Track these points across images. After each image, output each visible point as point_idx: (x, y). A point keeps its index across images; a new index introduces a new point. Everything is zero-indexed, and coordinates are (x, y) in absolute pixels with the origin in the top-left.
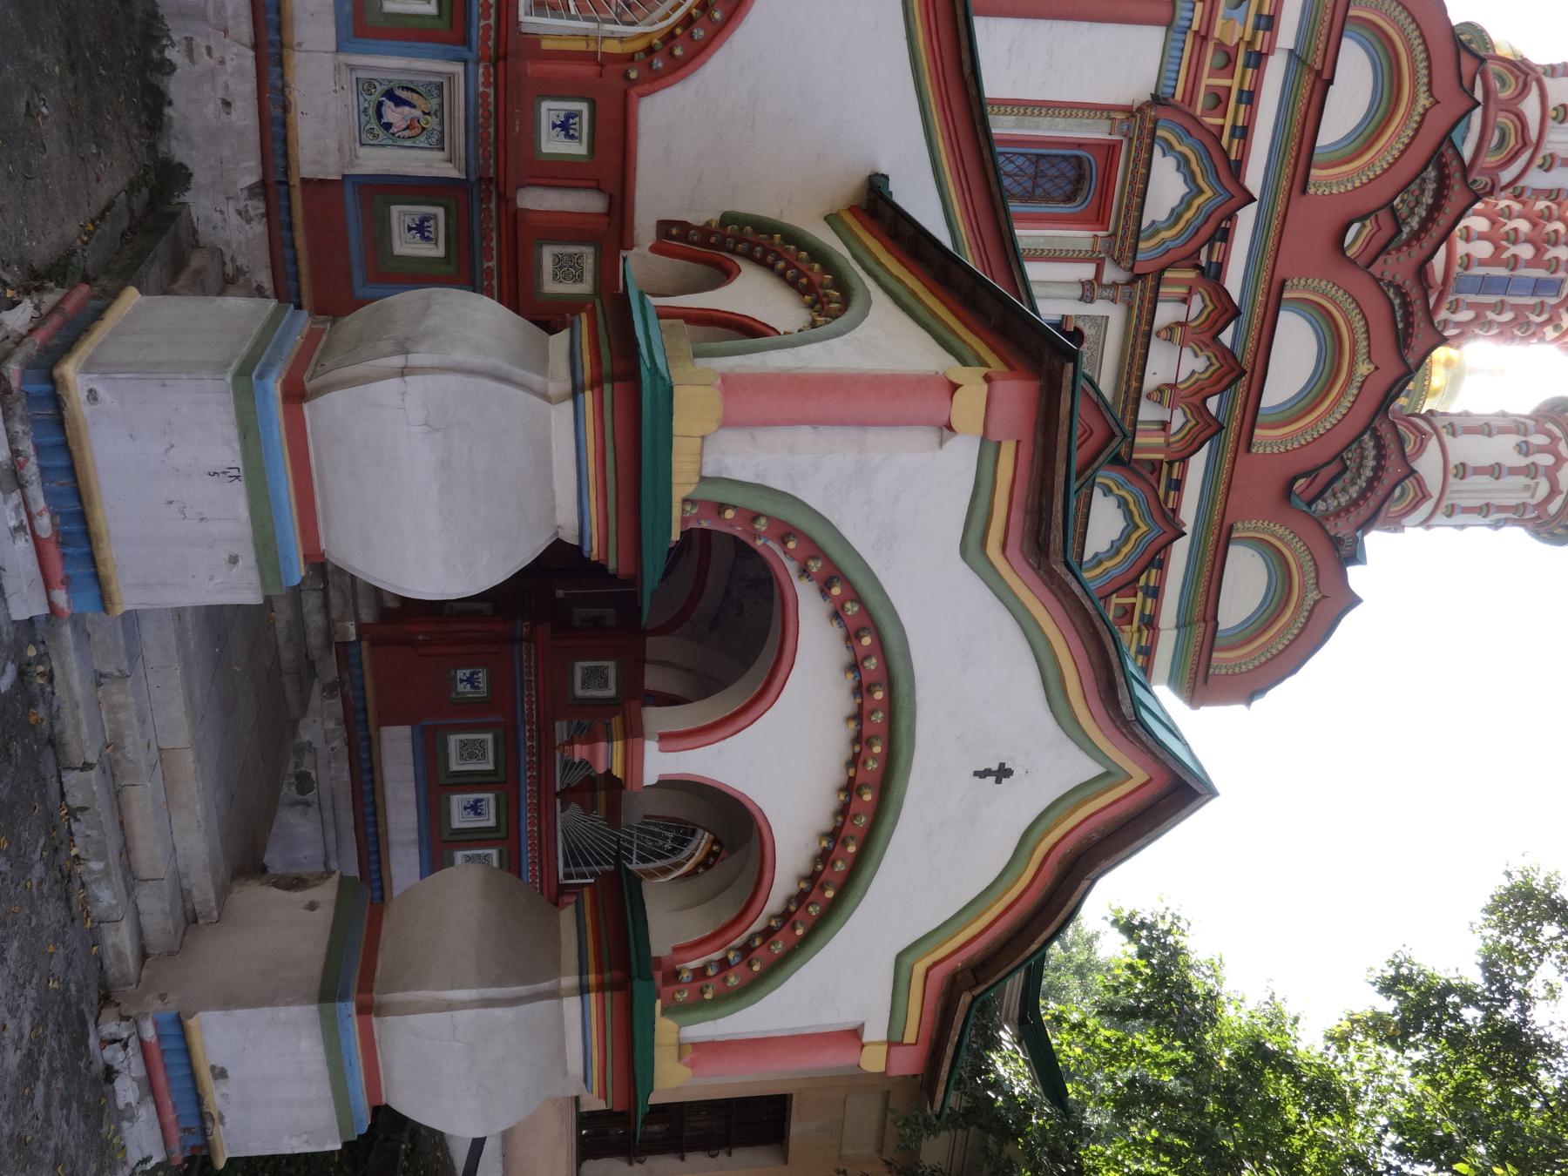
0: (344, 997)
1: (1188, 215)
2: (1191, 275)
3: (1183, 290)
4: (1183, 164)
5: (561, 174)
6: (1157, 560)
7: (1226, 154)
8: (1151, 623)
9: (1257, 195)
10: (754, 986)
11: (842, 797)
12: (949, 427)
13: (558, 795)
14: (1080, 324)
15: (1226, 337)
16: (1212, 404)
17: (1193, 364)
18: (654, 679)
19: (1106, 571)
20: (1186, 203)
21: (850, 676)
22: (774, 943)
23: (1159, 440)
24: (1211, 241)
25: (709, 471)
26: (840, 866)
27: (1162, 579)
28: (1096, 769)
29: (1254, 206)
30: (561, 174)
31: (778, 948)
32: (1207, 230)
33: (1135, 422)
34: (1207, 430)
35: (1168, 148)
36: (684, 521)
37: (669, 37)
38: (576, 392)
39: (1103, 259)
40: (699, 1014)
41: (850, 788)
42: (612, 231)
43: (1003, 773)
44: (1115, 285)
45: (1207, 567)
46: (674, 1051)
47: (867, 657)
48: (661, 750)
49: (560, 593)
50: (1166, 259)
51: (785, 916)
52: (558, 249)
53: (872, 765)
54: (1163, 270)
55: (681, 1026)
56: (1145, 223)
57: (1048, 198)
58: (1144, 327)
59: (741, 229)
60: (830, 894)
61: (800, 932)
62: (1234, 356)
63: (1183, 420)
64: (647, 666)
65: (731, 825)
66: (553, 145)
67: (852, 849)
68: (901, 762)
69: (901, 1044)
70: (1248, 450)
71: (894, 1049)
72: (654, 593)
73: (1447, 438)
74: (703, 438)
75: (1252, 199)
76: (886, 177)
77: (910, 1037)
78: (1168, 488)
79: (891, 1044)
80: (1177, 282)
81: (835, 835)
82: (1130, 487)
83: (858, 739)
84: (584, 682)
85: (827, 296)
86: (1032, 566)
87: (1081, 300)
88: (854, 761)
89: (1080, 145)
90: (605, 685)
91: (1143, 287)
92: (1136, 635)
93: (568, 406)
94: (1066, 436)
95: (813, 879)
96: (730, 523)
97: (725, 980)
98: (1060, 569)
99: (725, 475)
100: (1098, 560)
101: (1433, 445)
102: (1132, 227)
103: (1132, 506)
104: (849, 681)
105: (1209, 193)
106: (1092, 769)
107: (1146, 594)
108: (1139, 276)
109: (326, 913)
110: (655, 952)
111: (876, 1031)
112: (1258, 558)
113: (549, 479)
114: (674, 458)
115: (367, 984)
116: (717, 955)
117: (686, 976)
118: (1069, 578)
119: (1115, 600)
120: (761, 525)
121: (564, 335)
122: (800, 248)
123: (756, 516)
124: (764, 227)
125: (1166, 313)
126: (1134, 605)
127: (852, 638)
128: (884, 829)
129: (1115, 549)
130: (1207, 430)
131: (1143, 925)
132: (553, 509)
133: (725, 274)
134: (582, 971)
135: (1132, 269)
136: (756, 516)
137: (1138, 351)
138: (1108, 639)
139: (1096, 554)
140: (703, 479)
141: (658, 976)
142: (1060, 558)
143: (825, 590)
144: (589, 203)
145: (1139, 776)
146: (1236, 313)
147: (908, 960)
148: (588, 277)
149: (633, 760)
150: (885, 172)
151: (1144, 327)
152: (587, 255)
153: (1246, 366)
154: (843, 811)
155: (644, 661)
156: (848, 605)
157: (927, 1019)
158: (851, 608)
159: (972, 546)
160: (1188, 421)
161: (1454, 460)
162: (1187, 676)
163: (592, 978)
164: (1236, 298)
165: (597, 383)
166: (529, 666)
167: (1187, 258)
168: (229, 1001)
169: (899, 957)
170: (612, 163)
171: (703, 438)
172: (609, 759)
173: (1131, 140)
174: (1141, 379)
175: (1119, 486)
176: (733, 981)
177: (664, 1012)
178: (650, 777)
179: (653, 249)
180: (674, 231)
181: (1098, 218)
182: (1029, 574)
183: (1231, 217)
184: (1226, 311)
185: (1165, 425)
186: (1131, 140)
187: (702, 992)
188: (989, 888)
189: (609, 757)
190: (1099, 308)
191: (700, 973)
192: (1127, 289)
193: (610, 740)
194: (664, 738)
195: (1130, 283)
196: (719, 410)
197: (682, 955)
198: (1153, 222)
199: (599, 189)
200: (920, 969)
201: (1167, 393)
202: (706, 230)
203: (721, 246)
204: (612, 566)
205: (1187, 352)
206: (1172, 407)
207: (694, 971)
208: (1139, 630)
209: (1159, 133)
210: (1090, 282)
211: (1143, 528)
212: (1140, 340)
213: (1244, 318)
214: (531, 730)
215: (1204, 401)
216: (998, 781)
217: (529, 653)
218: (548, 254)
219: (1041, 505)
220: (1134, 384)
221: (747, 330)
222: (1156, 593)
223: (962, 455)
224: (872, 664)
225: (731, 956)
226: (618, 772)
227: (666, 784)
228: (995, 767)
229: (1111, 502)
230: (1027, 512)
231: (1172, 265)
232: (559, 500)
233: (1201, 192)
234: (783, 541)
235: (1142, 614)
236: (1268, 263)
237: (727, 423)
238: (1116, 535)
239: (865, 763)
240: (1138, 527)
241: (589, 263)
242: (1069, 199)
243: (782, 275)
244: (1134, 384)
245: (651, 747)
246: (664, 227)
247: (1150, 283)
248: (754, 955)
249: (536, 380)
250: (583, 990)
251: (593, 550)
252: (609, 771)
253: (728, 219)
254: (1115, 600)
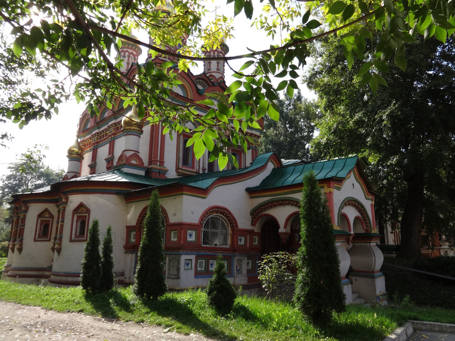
0: (373, 275)
37: (231, 223)
43: (353, 185)
66: (243, 243)
68: (352, 199)
73: (211, 71)
101: (213, 74)
109: (357, 278)
115: (370, 272)
134: (368, 243)
152: (254, 237)
161: (216, 71)
168: (375, 291)
169: (366, 199)
170: (245, 232)
191: (367, 226)
200: (368, 196)
218: (254, 244)
236: (202, 108)
246: (252, 225)
250: (370, 242)
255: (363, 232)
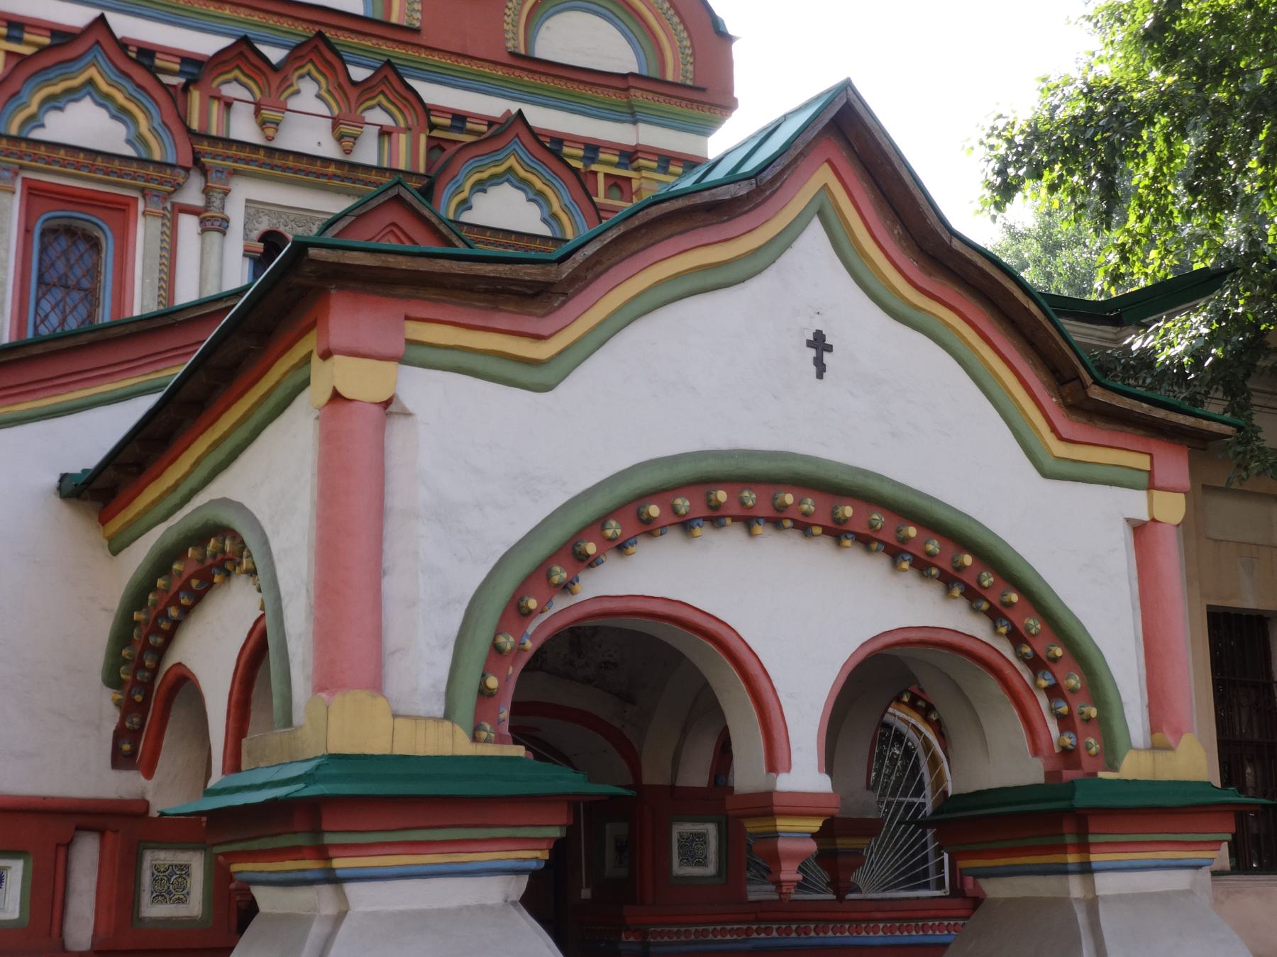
1: (120, 98)
2: (195, 96)
3: (215, 107)
4: (54, 103)
5: (48, 895)
6: (551, 147)
7: (43, 50)
8: (629, 155)
9: (94, 13)
10: (1082, 656)
11: (848, 543)
12: (387, 403)
13: (840, 898)
14: (255, 234)
15: (275, 55)
16: (358, 74)
17: (308, 96)
18: (696, 775)
19: (565, 208)
20: (104, 100)
21: (698, 531)
22: (1028, 630)
23: (403, 139)
24: (153, 71)
25: (438, 709)
26: (933, 546)
27: (574, 140)
28: (816, 227)
29: (112, 18)
30: (48, 895)
31: (1034, 624)
32: (140, 75)
33: (379, 170)
34: (391, 81)
35: (34, 121)
36: (500, 740)
38: (334, 879)
39: (173, 205)
40: (1116, 725)
41: (837, 532)
42: (124, 829)
43: (819, 343)
44: (206, 191)
45: (562, 85)
46: (1161, 756)
47: (675, 511)
48: (789, 769)
49: (586, 893)
50: (176, 127)
51: (994, 615)
52: (146, 897)
53: (808, 505)
54: (189, 131)
55: (1130, 746)
56: (129, 151)
57: (94, 272)
58: (261, 155)
59: (125, 662)
60: (968, 560)
61: (1014, 597)
62: (299, 46)
63: (378, 111)
64: (679, 784)
65: (883, 682)
67: (912, 531)
69: (1151, 473)
70: (416, 31)
71: (1158, 482)
72: (591, 780)
74: (395, 716)
75: (101, 20)
76: (64, 477)
77: (1142, 462)
78: (462, 130)
79: (1151, 486)
80: (205, 114)
81: (895, 553)
82: (460, 177)
83: (776, 522)
84: (699, 864)
85: (215, 554)
86: (564, 303)
87: (224, 234)
88: (804, 527)
89: (27, 231)
90: (702, 837)
91: (210, 156)
92: (644, 173)
93: (350, 888)
94: (400, 258)
95: (949, 580)
96: (504, 681)
97: (1073, 691)
98: (567, 268)
99: (443, 688)
100: (551, 218)
102: (134, 168)
103: (485, 175)
104: (704, 533)
105: (92, 72)
106: (815, 234)
107: (594, 160)
108: (196, 161)
110: (1040, 778)
111: (1136, 504)
112: (549, 23)
113: (443, 913)
114: (421, 751)
116: (1043, 701)
117: (1069, 740)
118: (579, 257)
119: (600, 199)
120: (507, 642)
121: (259, 893)
122: (152, 587)
123: (496, 649)
124: (124, 633)
125: (243, 128)
126: (607, 175)
127: (650, 529)
128: (887, 490)
129: (537, 197)
130: (391, 81)
131: (1001, 172)
132: (483, 907)
133: (184, 682)
134: (1063, 871)
135: (187, 170)
136: (496, 649)
137: (290, 163)
138: (655, 211)
139: (544, 220)
140: (448, 716)
141: (1068, 775)
142: (554, 268)
143: (590, 562)
144: (86, 859)
145: (824, 176)
146: (245, 43)
147: (1049, 464)
148: (182, 858)
149: (801, 805)
150: (54, 480)
151: (261, 155)
152: (155, 859)
153: (311, 31)
154: (865, 541)
155: (673, 787)
156: (609, 533)
157: (1120, 440)
158: (613, 529)
159: (538, 377)
160: (379, 105)
162: (696, 112)
163: (1072, 858)
164: (226, 42)
165: (323, 852)
166: (678, 933)
167: (174, 100)
169: (1046, 474)
171: (395, 716)
172: (800, 836)
173: (22, 167)
174: (327, 161)
175: (458, 190)
176: (1074, 681)
177: (1114, 768)
178: (819, 783)
179: (149, 774)
180: (126, 747)
181: (120, 210)
182: (573, 306)
183: (123, 45)
184: (243, 54)
185: (384, 133)
186: (22, 167)
187: (1088, 720)
188: (961, 362)
189: (797, 836)
190: (235, 211)
191: (1065, 722)
192: (213, 175)
193: (775, 835)
194: (772, 767)
195: (204, 171)
196: (362, 695)
197: (1043, 744)
198: (129, 142)
199: (69, 845)
200: (1060, 449)
201: (344, 129)
202: (127, 708)
203: (147, 687)
204: (556, 833)
205: (293, 104)
206: (362, 123)
207: (1062, 731)
208: (638, 169)
209: (14, 131)
210: (202, 221)
211: (512, 161)
212: (277, 162)
213: (252, 32)
214: (758, 931)
215: (354, 84)
216: (829, 348)
217: (661, 934)
218: (152, 910)
219: (486, 291)
220: (332, 169)
221: (257, 655)
222: (592, 148)
223: (422, 389)
224: (683, 504)
225: (1044, 683)
226: (815, 825)
227: (830, 764)
228: (812, 353)
229: (479, 200)
230: (495, 309)
231: (183, 119)
232: (471, 900)
233: (91, 82)
234: (528, 614)
235: (618, 165)
237: (377, 685)
238: (519, 196)
239: (806, 514)
240: (511, 169)
241: (165, 857)
242: (95, 245)
243: (187, 611)
244: (332, 169)
245: (785, 783)
246: (120, 760)
247: (204, 147)
248: (1042, 654)
249: (317, 931)
250: (1086, 870)
251: (536, 856)
252: (814, 836)
253: (112, 679)
254: (600, 199)
255: (1031, 772)
